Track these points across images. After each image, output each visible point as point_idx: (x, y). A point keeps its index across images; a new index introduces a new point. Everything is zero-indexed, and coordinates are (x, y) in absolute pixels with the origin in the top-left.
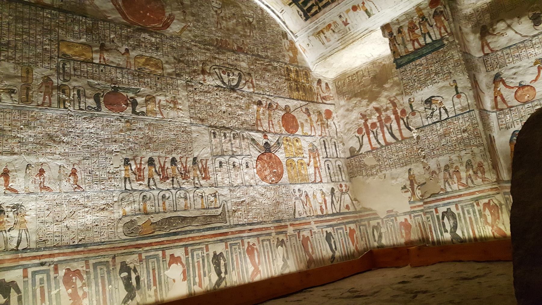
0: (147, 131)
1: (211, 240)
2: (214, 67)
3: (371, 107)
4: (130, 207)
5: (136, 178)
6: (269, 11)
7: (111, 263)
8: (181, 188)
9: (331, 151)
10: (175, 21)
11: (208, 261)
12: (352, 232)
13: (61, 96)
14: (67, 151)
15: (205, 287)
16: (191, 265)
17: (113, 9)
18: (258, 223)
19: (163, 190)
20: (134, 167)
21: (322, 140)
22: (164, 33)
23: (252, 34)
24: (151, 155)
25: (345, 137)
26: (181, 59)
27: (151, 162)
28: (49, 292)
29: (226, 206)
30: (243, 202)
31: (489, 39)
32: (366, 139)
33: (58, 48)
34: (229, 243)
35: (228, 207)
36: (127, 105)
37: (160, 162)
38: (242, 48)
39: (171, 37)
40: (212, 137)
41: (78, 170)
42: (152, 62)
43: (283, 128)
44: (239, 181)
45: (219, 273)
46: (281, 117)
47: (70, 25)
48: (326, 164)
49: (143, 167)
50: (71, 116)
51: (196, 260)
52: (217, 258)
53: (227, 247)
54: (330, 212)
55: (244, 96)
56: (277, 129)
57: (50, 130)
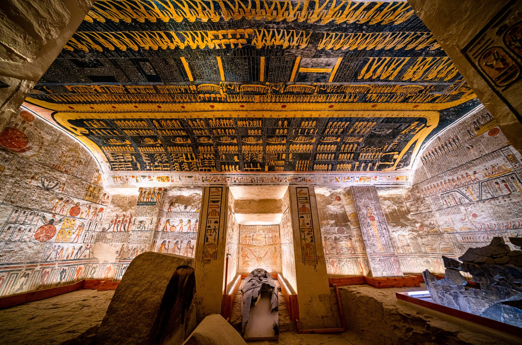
3: (122, 213)
6: (95, 159)
9: (92, 227)
25: (104, 222)
31: (172, 207)
32: (113, 226)
56: (65, 213)
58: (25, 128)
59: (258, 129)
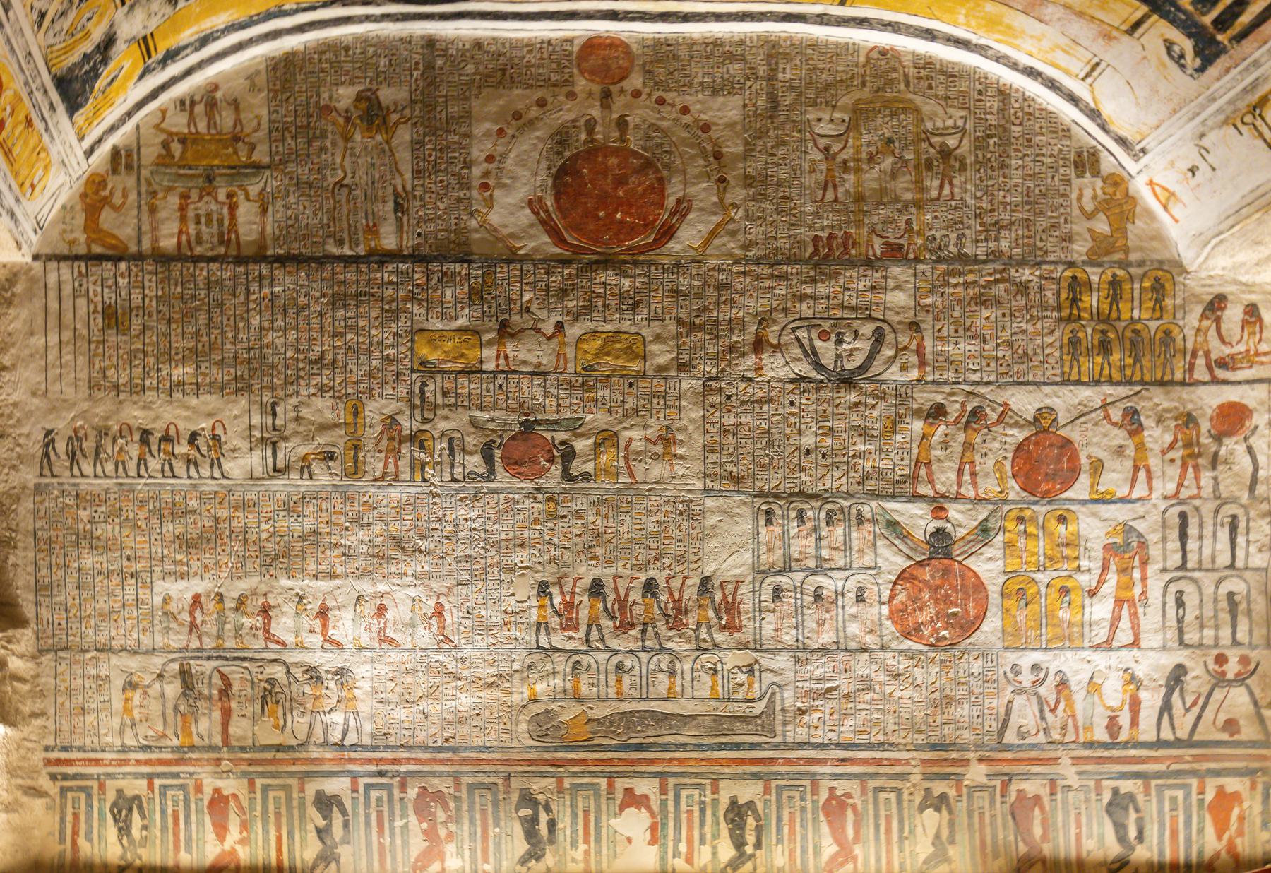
0: (592, 519)
1: (727, 770)
2: (793, 325)
4: (545, 685)
5: (561, 624)
6: (1033, 88)
7: (501, 788)
8: (662, 650)
9: (1211, 544)
10: (690, 216)
11: (714, 814)
12: (1224, 801)
13: (417, 455)
14: (426, 568)
15: (702, 864)
16: (671, 816)
17: (532, 226)
18: (869, 746)
19: (618, 652)
20: (557, 600)
21: (1176, 510)
22: (660, 259)
23: (946, 191)
24: (597, 572)
26: (697, 321)
27: (596, 589)
28: (392, 821)
29: (778, 697)
30: (829, 690)
33: (412, 349)
34: (774, 783)
35: (783, 700)
36: (551, 460)
37: (616, 588)
38: (900, 247)
39: (677, 265)
40: (762, 522)
41: (447, 606)
42: (618, 346)
43: (1012, 482)
44: (827, 637)
45: (739, 844)
46: (1013, 448)
47: (435, 291)
48: (1173, 588)
49: (577, 599)
50: (436, 496)
51: (683, 807)
52: (737, 813)
53: (767, 791)
54: (1150, 736)
55: (882, 397)
56: (989, 486)
57: (397, 528)
58: (622, 124)
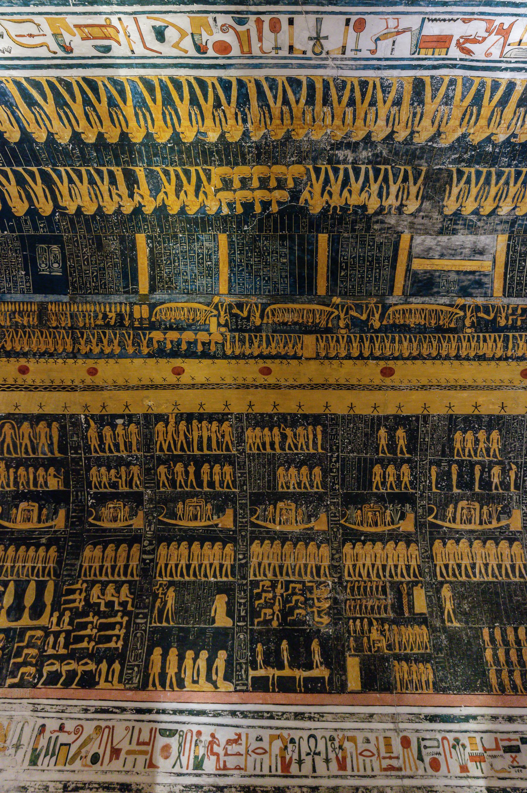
59: (309, 461)
